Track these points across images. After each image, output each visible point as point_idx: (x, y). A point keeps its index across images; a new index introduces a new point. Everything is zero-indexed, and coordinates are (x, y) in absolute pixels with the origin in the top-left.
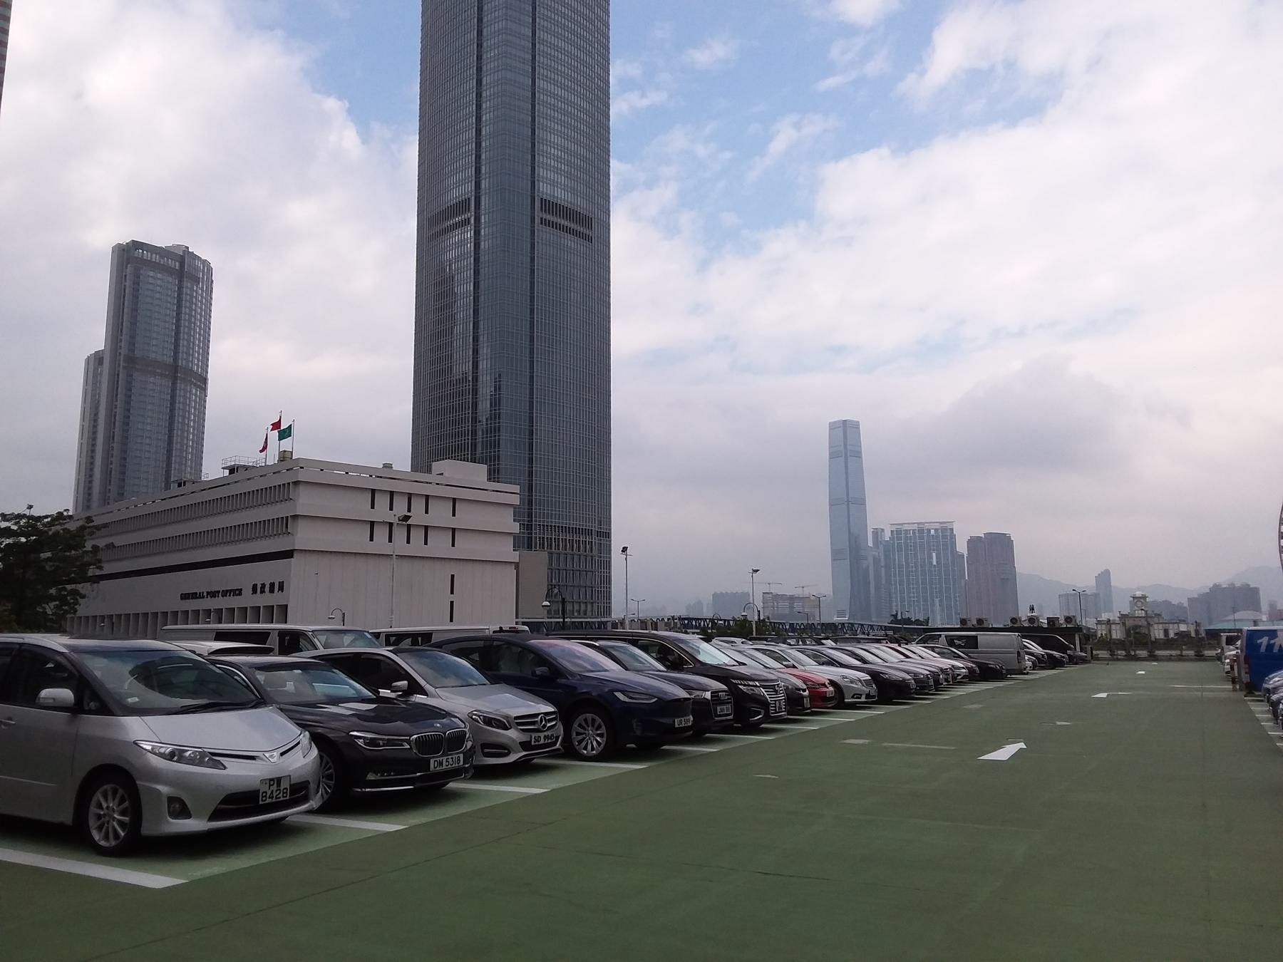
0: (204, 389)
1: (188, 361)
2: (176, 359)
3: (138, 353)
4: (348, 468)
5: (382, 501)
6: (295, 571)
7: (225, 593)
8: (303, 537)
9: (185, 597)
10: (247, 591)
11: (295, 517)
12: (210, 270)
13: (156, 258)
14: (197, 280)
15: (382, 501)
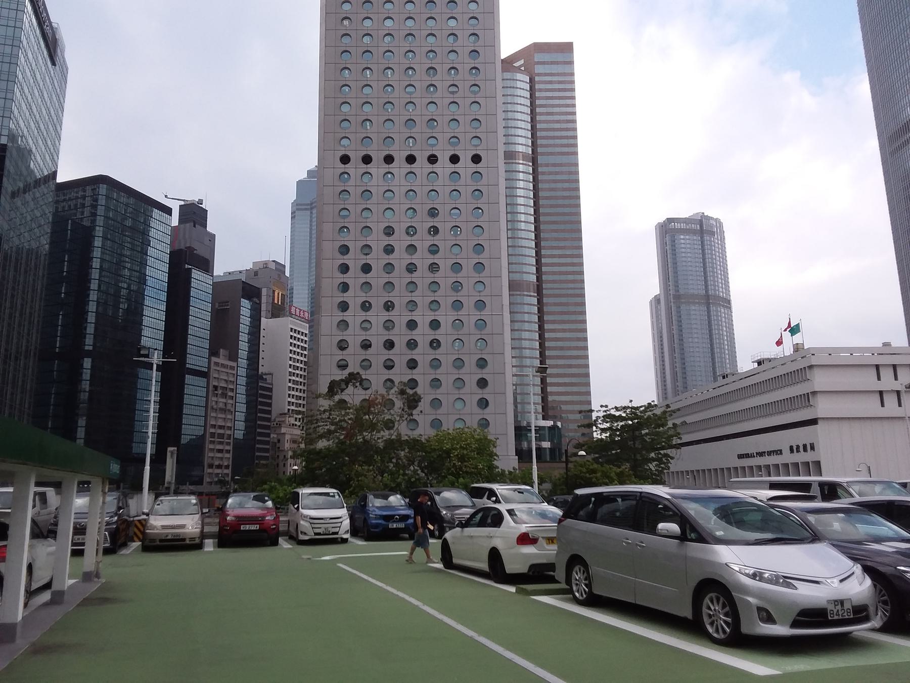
0: (730, 308)
1: (715, 290)
2: (707, 291)
3: (682, 292)
4: (851, 351)
5: (887, 374)
6: (820, 434)
7: (770, 453)
8: (823, 407)
9: (741, 456)
10: (786, 451)
11: (814, 393)
12: (721, 224)
13: (683, 226)
14: (712, 233)
15: (887, 374)
